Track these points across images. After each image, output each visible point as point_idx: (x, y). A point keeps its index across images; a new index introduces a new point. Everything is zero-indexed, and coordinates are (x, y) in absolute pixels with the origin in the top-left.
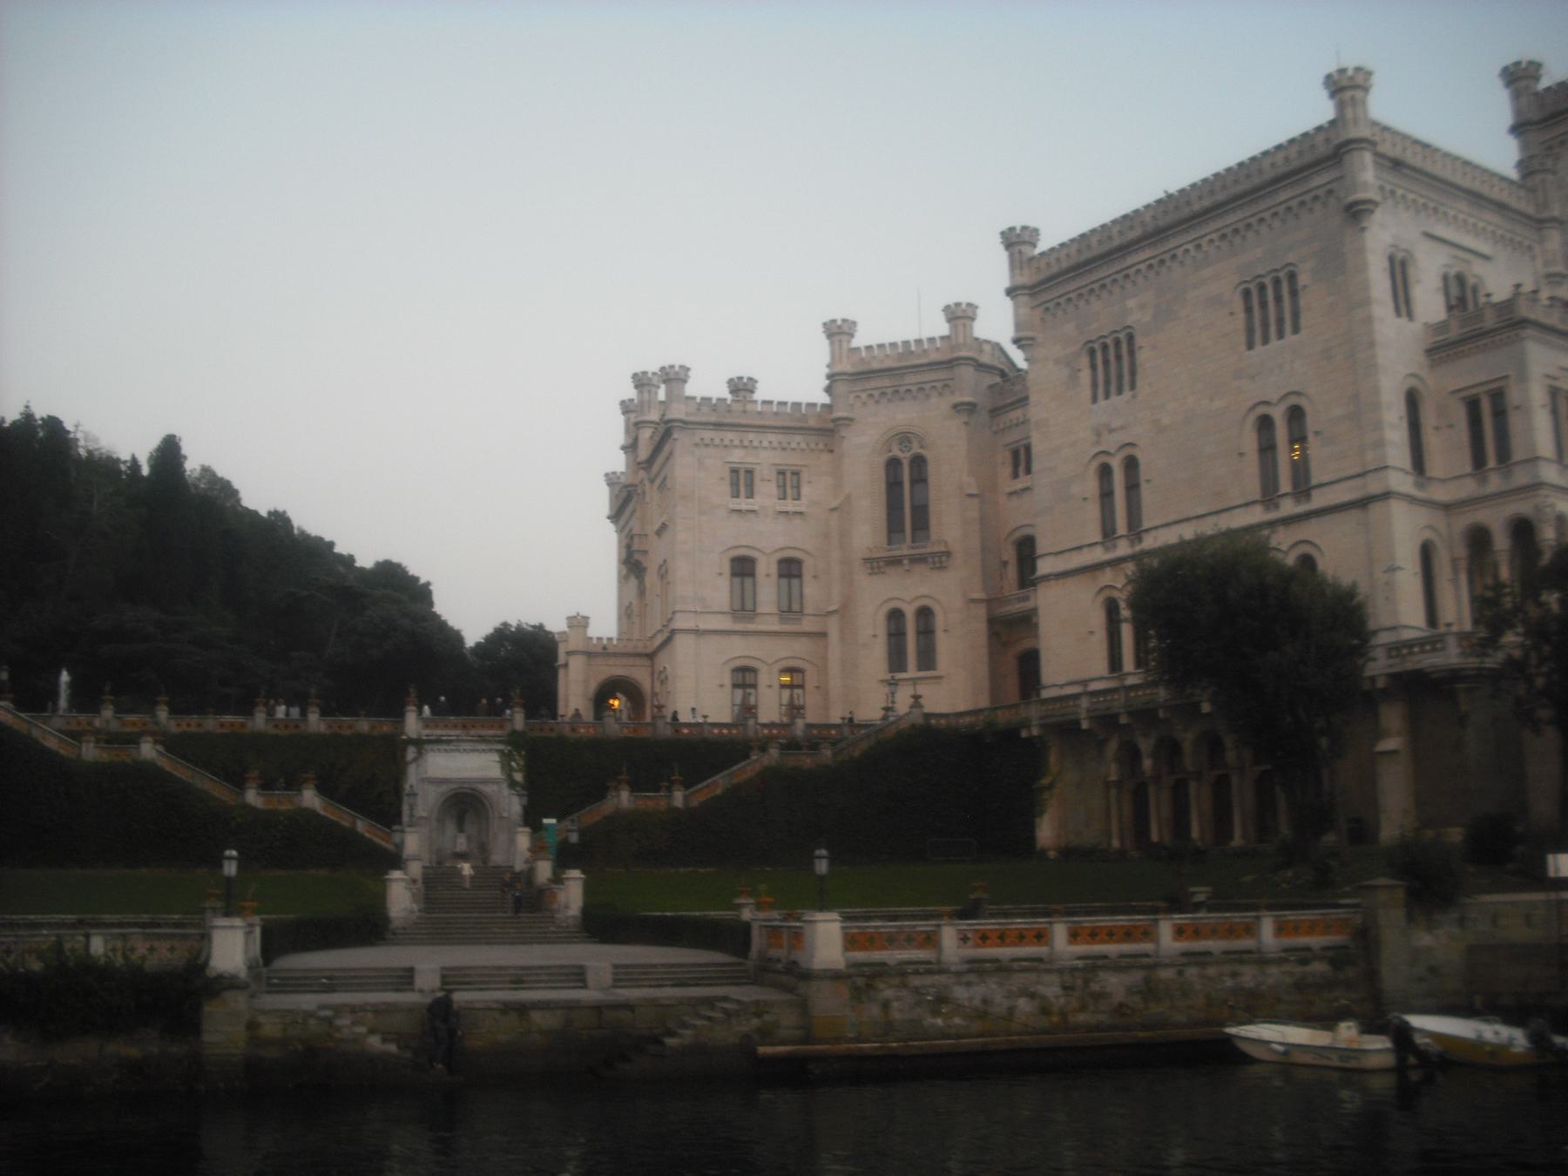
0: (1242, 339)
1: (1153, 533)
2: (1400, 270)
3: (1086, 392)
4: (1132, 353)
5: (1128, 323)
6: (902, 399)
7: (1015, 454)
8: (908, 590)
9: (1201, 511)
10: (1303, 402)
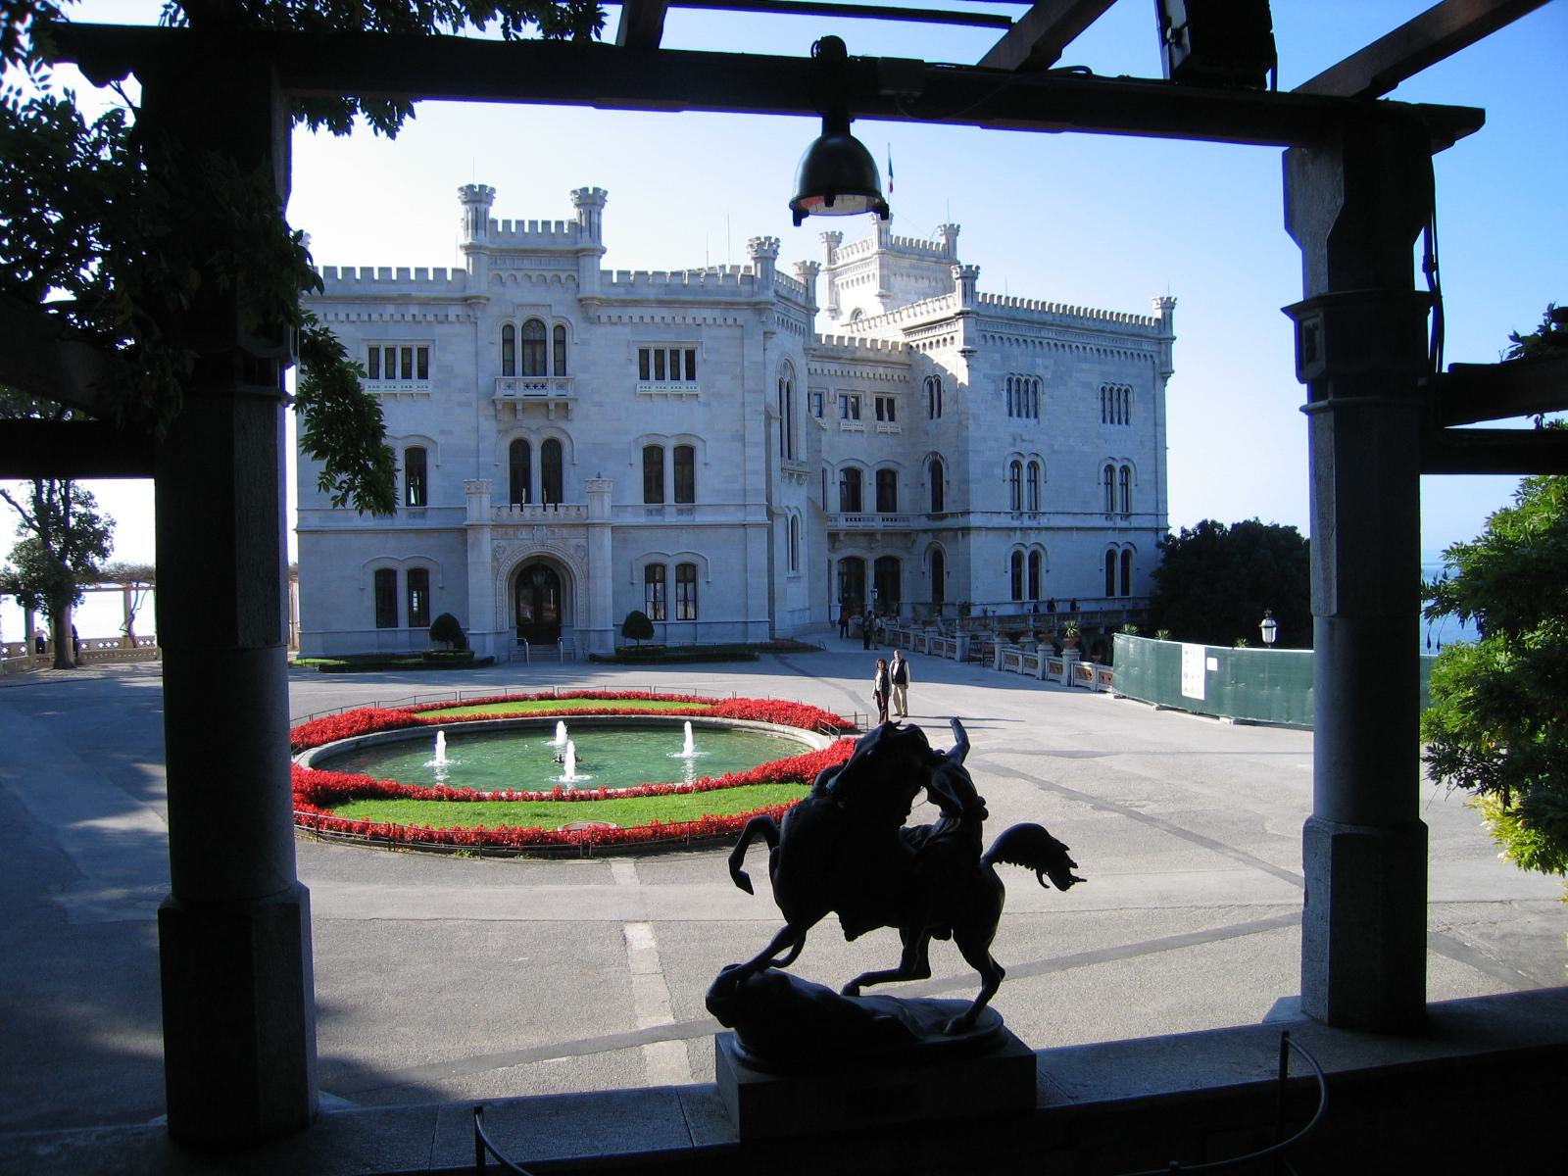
3: (1006, 410)
4: (1035, 392)
6: (787, 327)
9: (1076, 510)
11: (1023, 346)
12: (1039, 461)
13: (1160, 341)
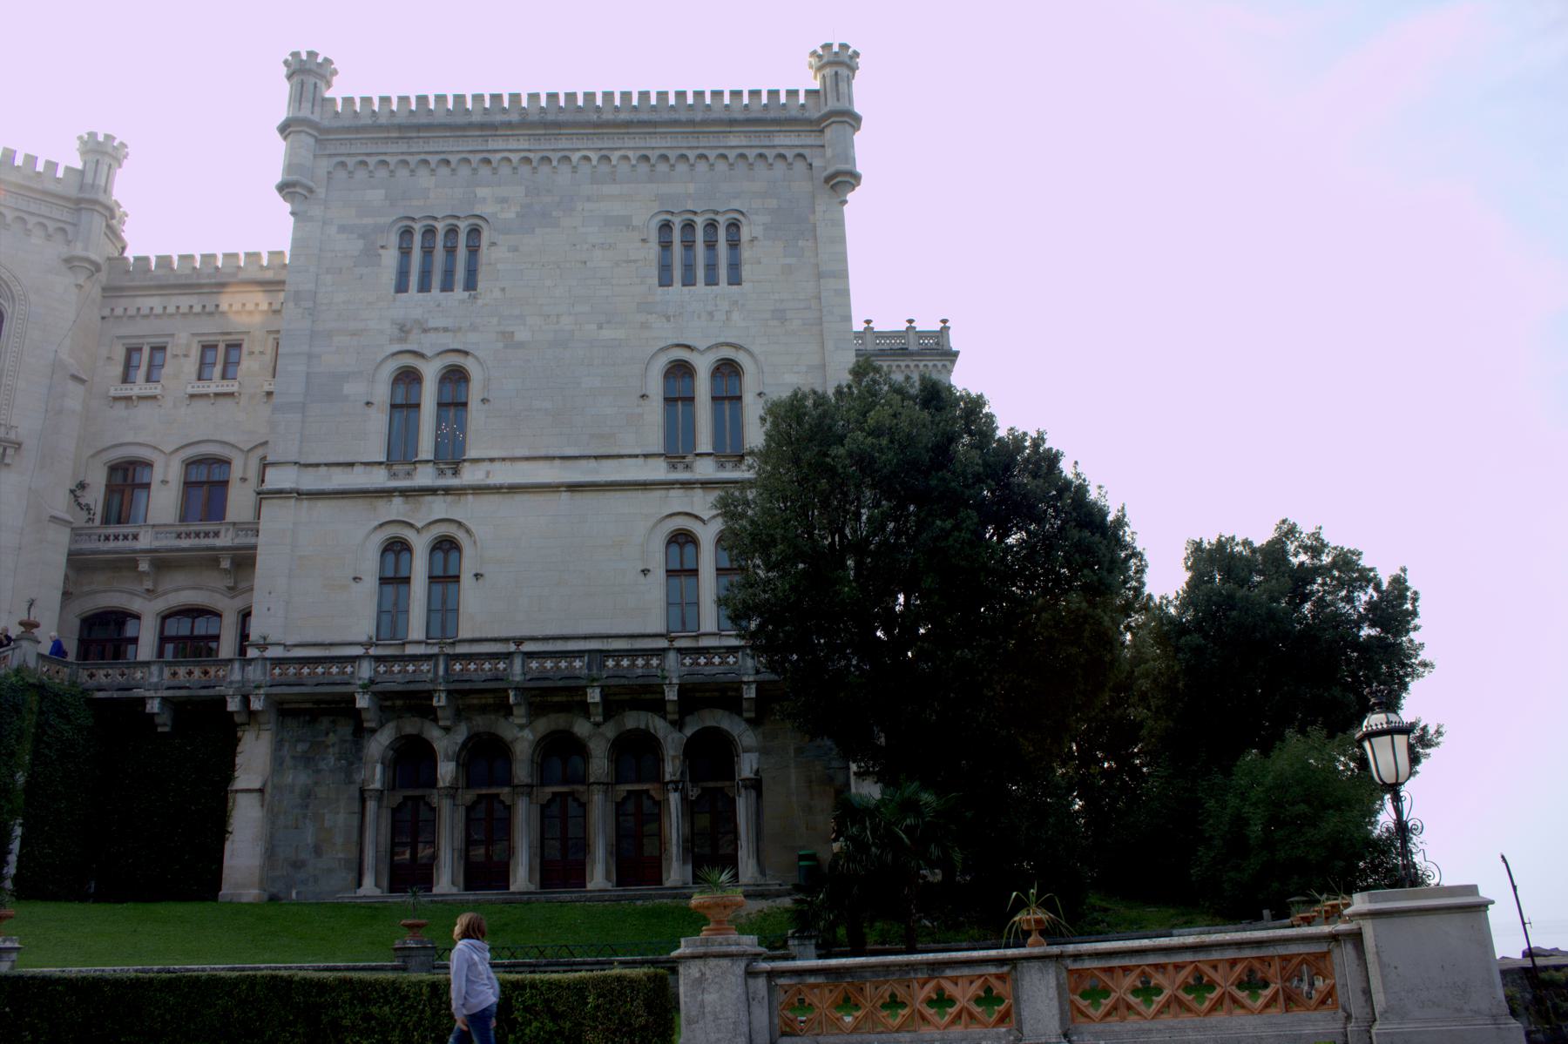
0: (654, 272)
1: (486, 466)
3: (389, 275)
4: (473, 250)
5: (478, 213)
10: (741, 358)
11: (444, 171)
12: (470, 364)
13: (817, 125)
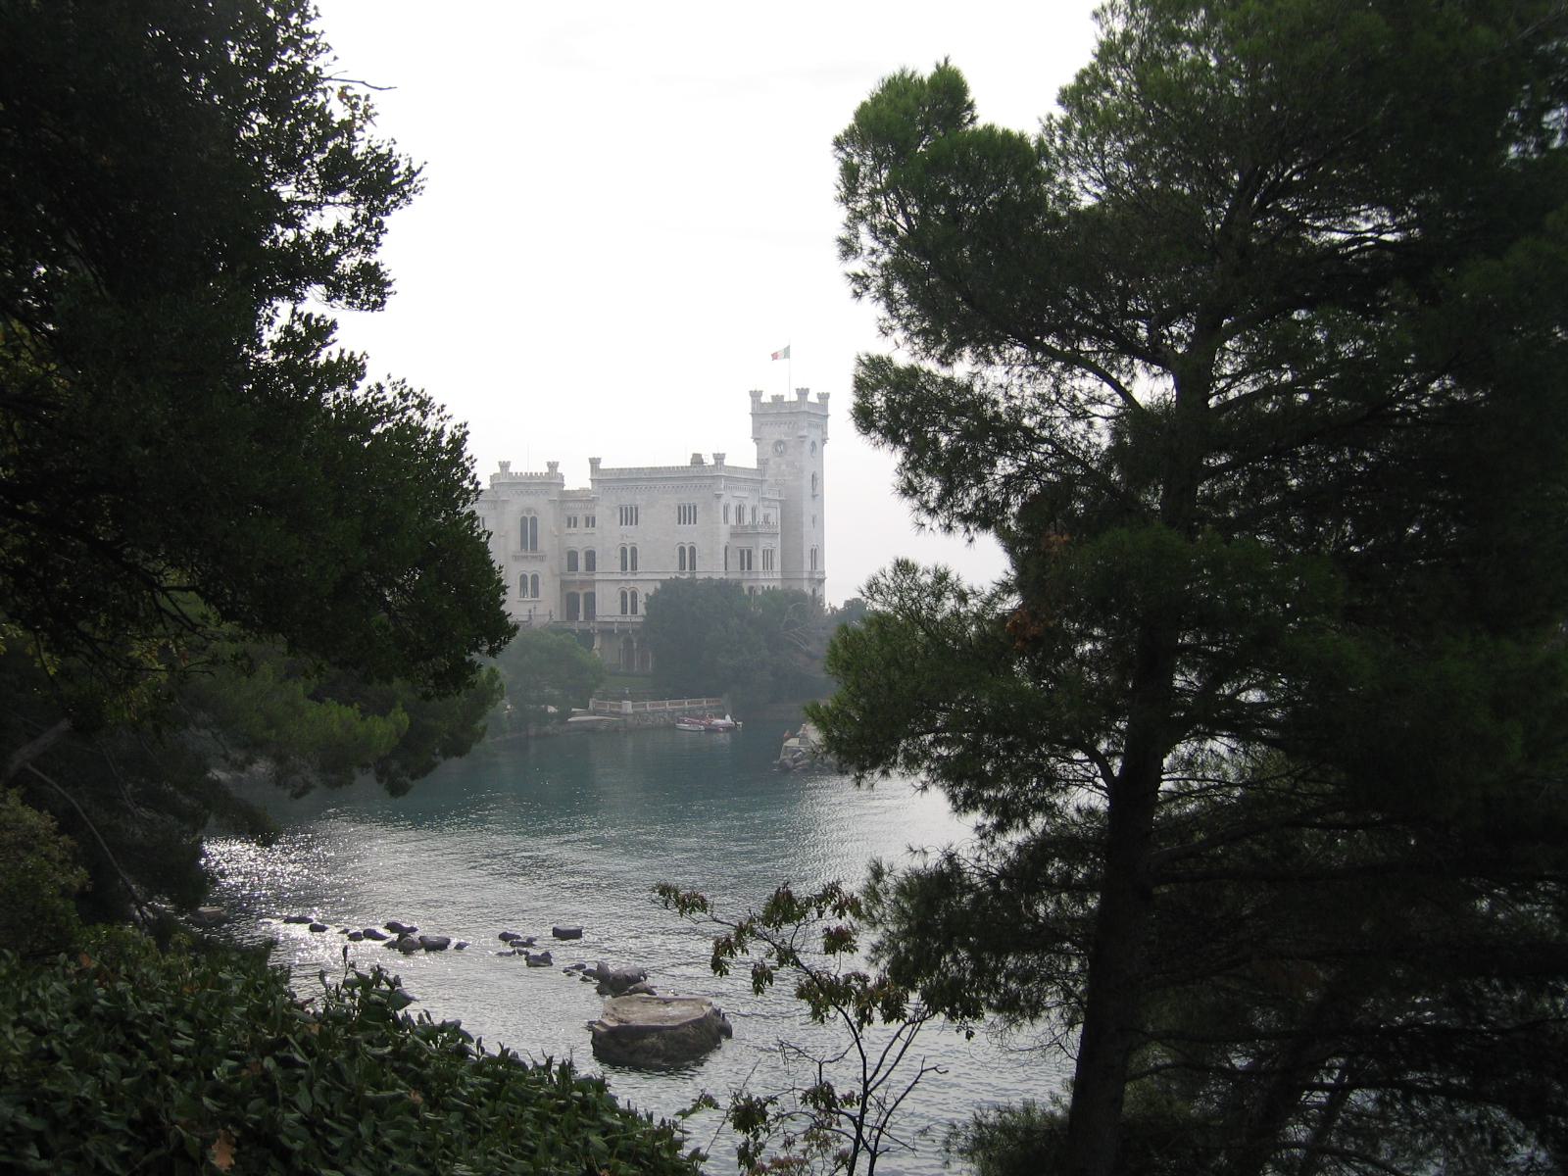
2: (726, 508)
7: (569, 519)
8: (530, 569)
